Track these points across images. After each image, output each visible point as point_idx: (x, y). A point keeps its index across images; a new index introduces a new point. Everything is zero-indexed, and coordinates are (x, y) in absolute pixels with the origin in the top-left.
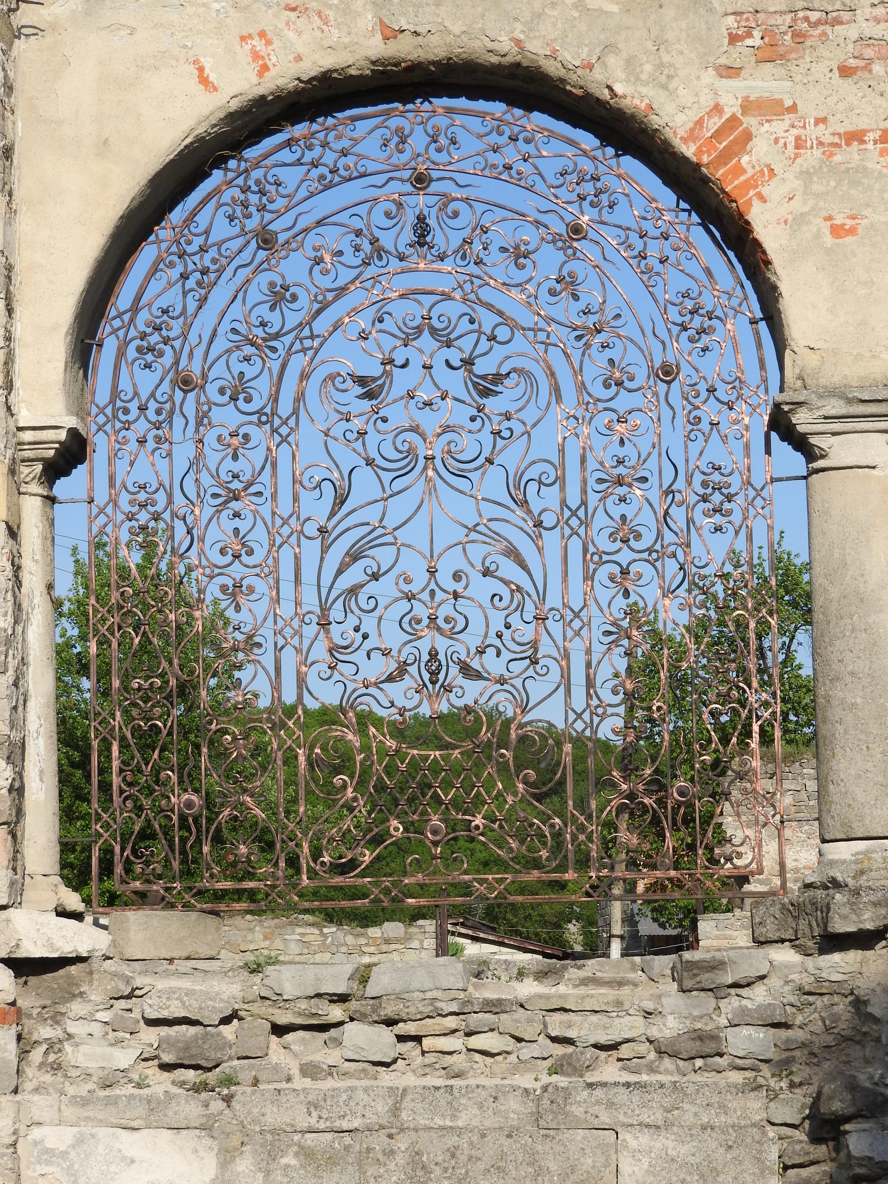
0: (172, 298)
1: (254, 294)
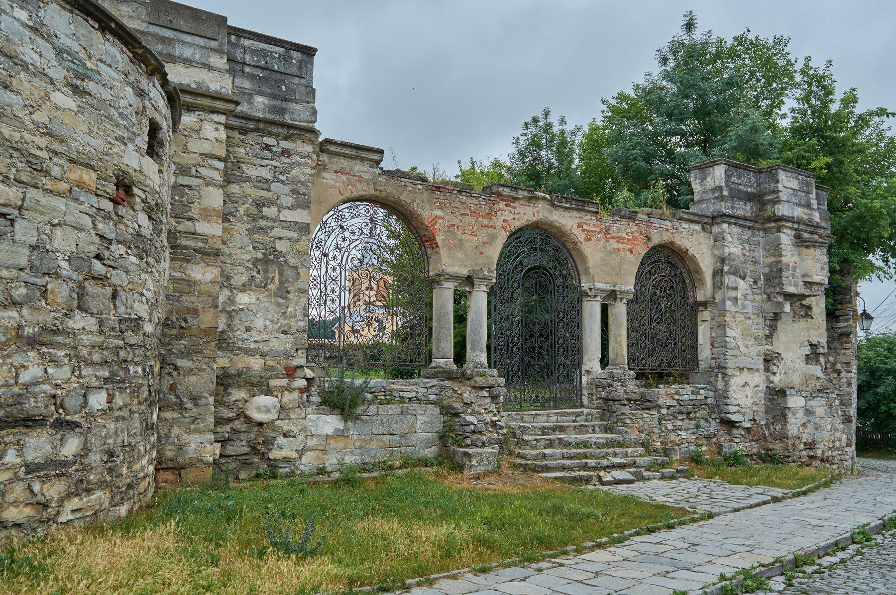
0: (323, 237)
1: (339, 239)
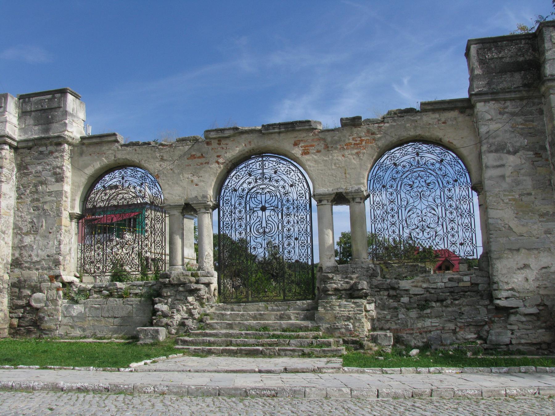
1: (393, 172)
